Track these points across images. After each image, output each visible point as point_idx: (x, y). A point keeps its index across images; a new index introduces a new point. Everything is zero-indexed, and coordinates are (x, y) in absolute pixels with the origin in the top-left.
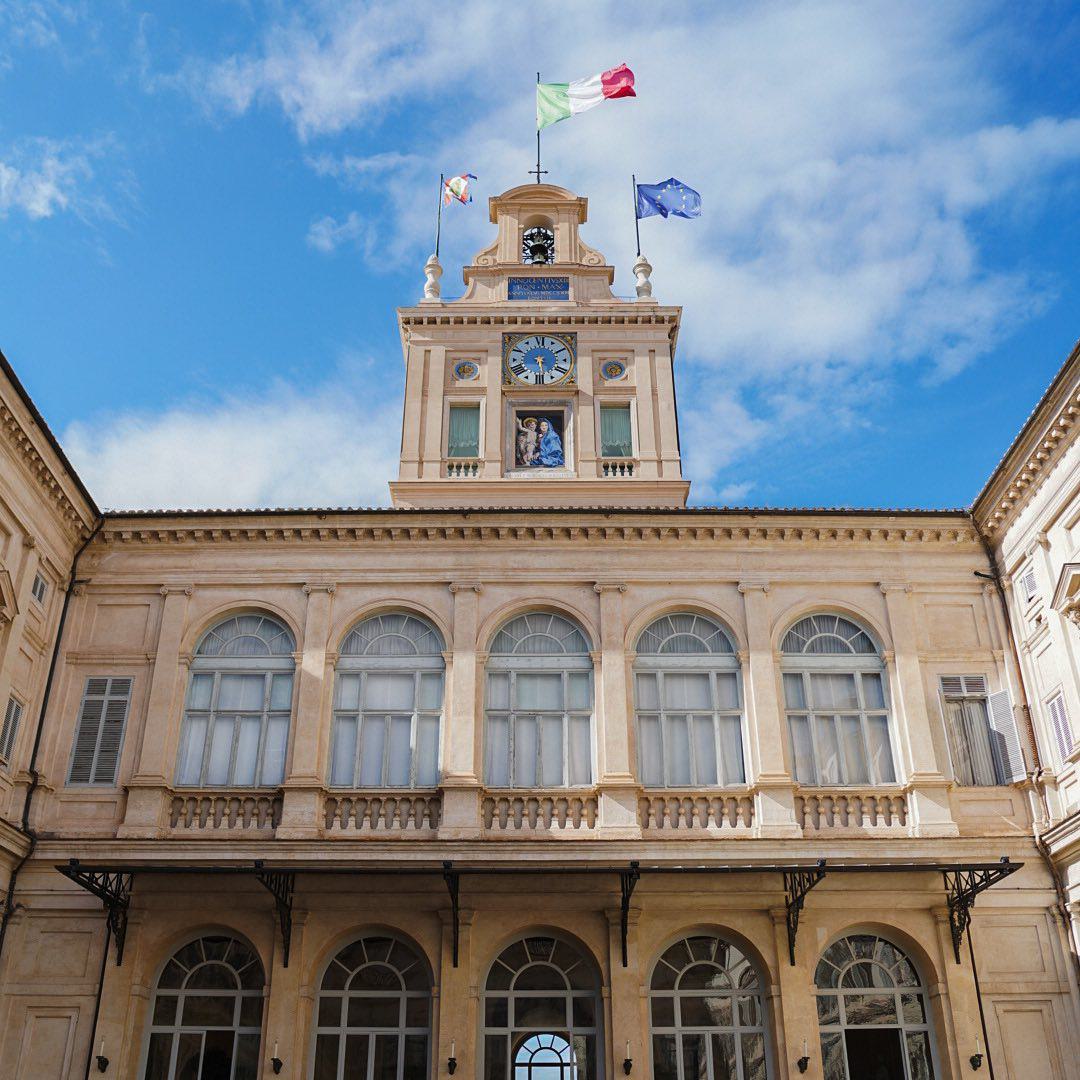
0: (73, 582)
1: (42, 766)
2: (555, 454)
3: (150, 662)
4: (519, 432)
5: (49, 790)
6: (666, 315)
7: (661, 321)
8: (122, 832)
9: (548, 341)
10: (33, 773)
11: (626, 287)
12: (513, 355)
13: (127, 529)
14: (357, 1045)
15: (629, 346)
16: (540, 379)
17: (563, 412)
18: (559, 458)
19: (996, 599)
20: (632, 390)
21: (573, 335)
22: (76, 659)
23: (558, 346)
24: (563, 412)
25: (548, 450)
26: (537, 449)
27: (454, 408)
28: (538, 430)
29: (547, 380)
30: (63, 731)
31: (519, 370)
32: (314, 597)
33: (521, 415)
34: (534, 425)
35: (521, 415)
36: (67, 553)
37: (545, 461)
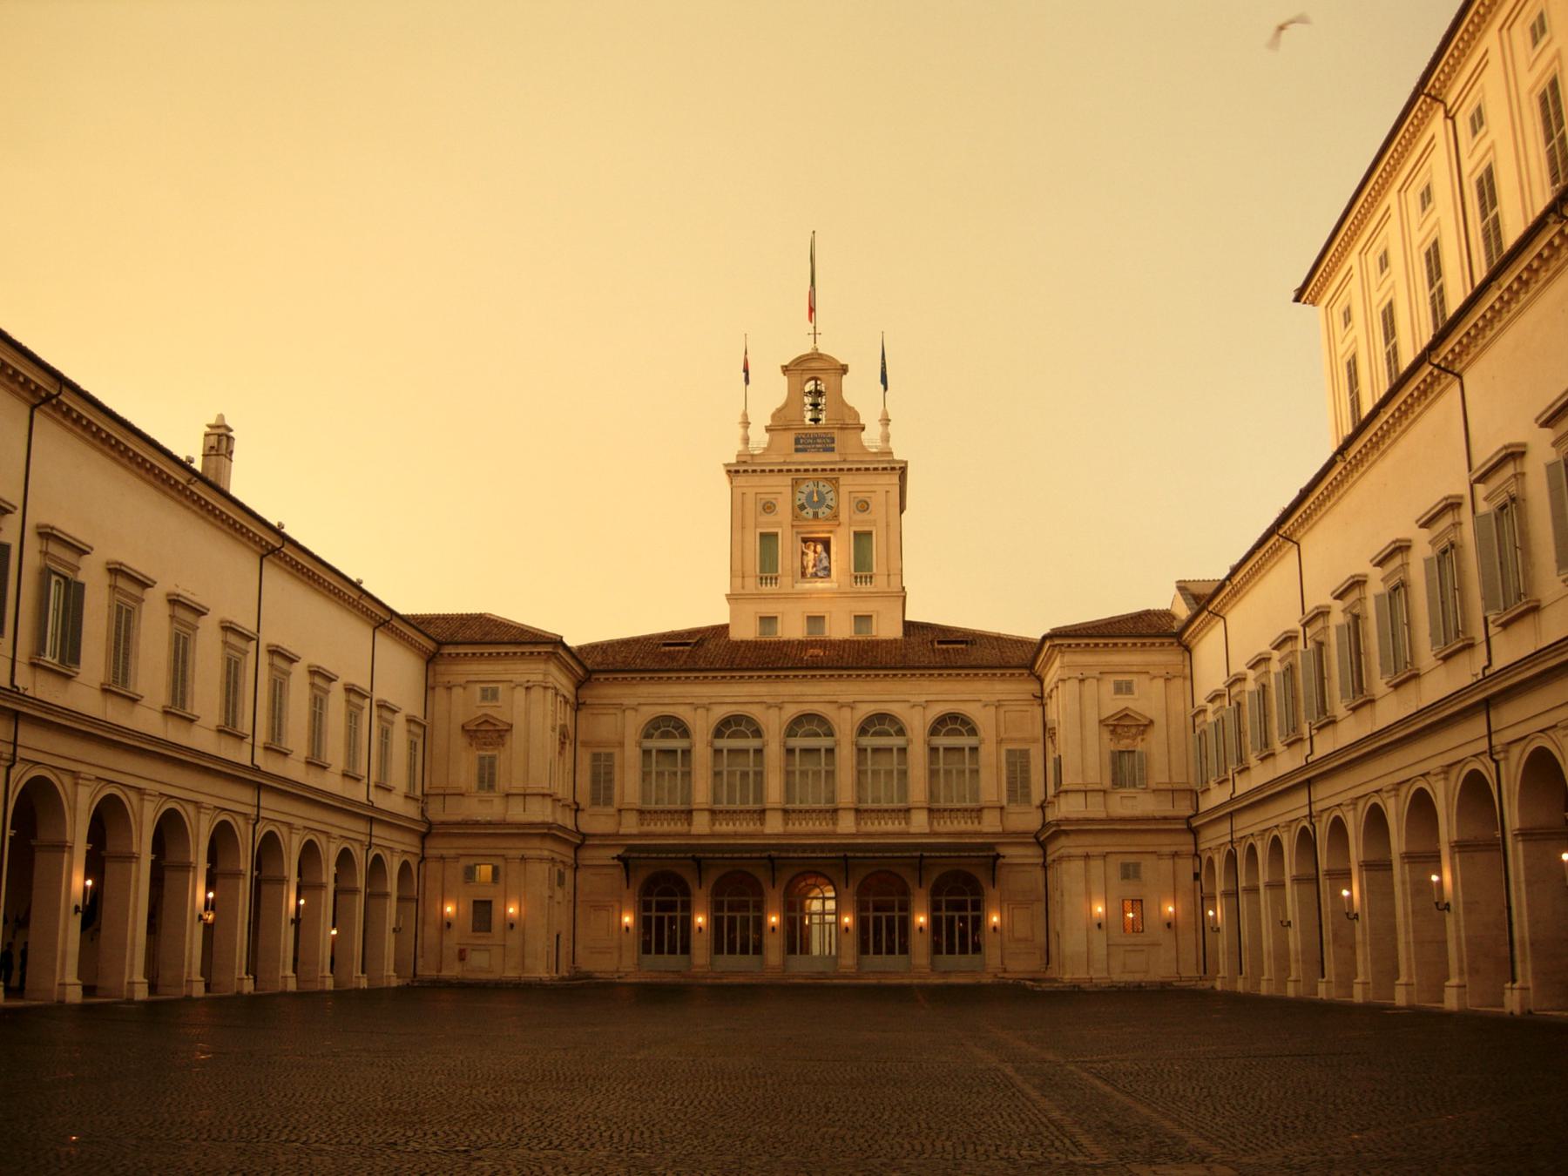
0: (578, 704)
1: (578, 799)
2: (825, 568)
3: (621, 744)
4: (803, 553)
5: (583, 810)
6: (897, 466)
7: (893, 469)
8: (622, 831)
9: (821, 484)
10: (575, 803)
11: (871, 438)
12: (799, 495)
13: (602, 677)
14: (732, 921)
15: (874, 488)
16: (816, 515)
17: (829, 538)
18: (828, 569)
19: (1041, 709)
20: (874, 523)
21: (837, 479)
22: (585, 744)
23: (828, 488)
24: (829, 538)
25: (821, 566)
26: (815, 566)
27: (762, 535)
28: (815, 552)
29: (820, 515)
30: (584, 780)
31: (802, 507)
32: (699, 711)
33: (805, 541)
34: (812, 548)
35: (805, 541)
36: (572, 689)
37: (819, 574)
